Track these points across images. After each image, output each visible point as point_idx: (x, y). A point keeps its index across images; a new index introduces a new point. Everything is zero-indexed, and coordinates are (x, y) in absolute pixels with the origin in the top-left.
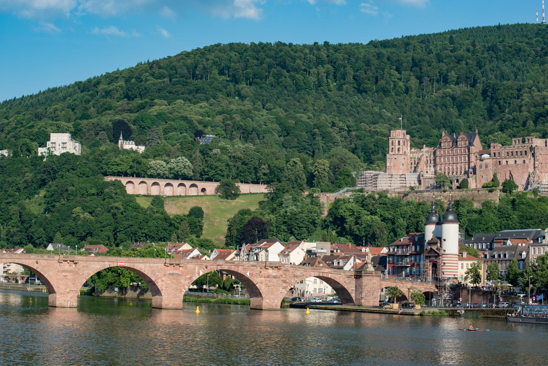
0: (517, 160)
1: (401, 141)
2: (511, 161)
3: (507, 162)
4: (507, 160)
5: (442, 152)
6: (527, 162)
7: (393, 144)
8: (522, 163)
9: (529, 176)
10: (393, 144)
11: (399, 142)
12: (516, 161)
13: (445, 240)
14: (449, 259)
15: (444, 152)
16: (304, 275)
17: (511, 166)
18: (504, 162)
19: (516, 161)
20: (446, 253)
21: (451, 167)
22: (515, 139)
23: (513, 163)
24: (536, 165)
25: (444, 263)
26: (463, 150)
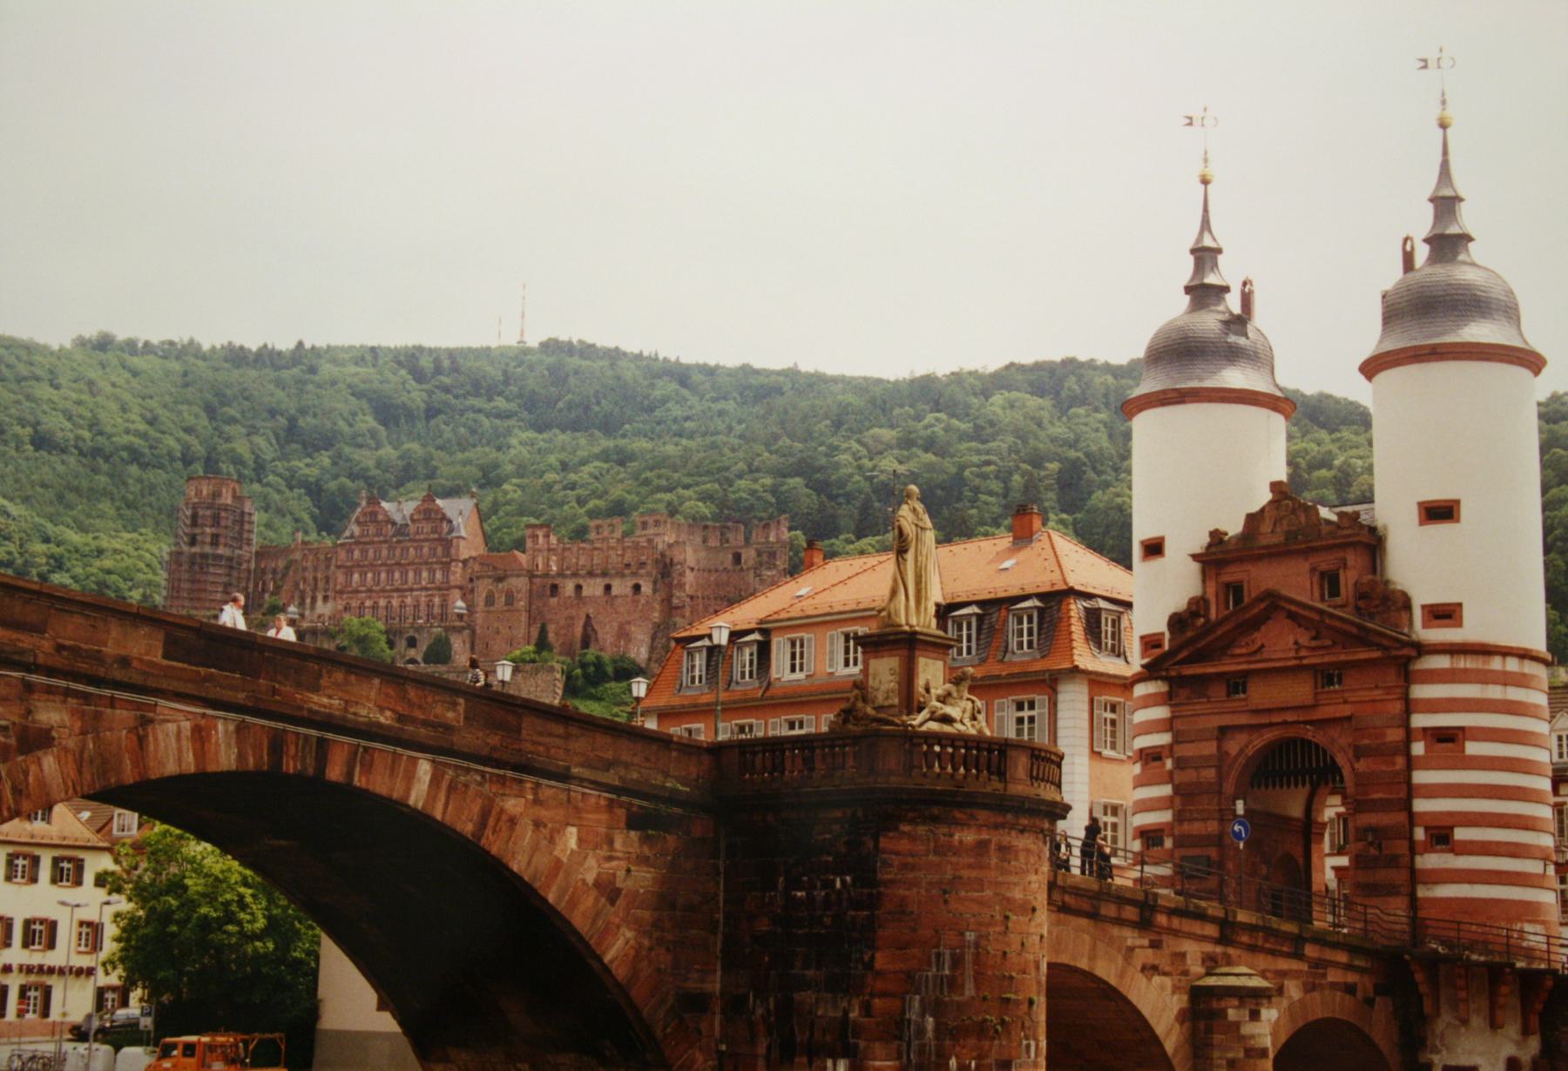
2: (593, 588)
3: (579, 588)
4: (581, 581)
5: (357, 554)
6: (646, 588)
8: (629, 591)
9: (653, 638)
12: (608, 588)
13: (1439, 512)
14: (1495, 692)
15: (364, 552)
17: (593, 599)
18: (569, 587)
19: (608, 588)
20: (1470, 631)
21: (382, 603)
23: (599, 591)
24: (675, 601)
25: (1447, 737)
26: (426, 550)
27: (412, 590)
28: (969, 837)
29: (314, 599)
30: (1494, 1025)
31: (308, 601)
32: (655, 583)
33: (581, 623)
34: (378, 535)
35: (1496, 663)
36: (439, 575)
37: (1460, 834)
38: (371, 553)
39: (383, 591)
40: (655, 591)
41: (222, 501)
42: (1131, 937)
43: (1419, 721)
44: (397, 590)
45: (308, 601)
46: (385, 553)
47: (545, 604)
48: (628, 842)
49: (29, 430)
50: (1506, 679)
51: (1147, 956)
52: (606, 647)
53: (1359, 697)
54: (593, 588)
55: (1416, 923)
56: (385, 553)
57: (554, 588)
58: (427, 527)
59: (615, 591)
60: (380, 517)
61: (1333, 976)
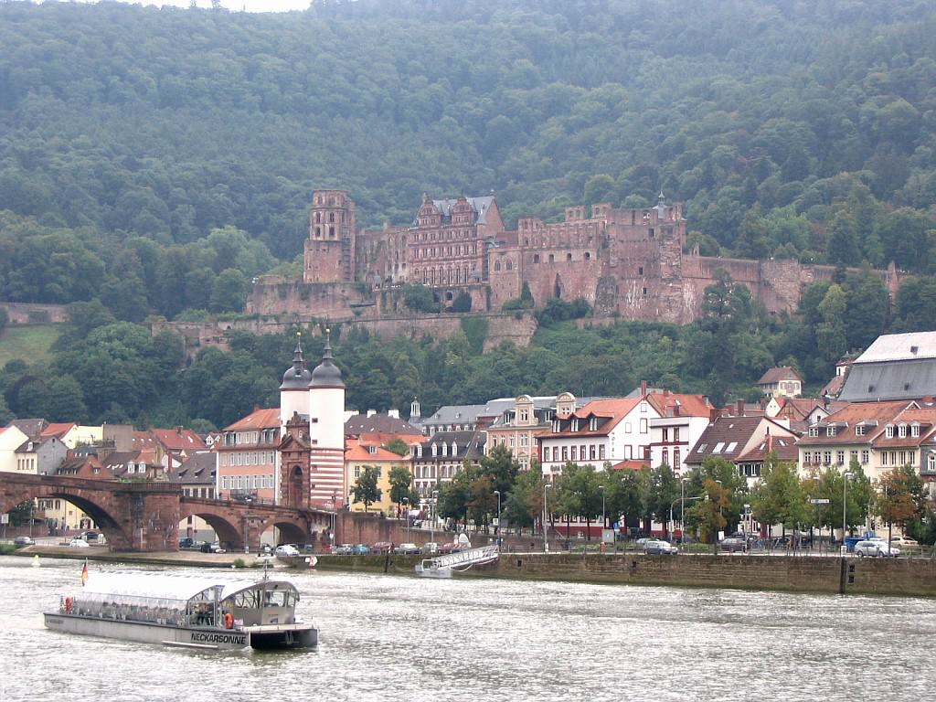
0: (574, 253)
1: (336, 214)
2: (560, 257)
4: (553, 253)
6: (593, 256)
7: (318, 221)
9: (597, 290)
10: (318, 221)
11: (332, 215)
13: (315, 421)
15: (425, 236)
16: (25, 492)
18: (545, 256)
19: (570, 256)
21: (437, 268)
22: (570, 209)
23: (564, 258)
25: (315, 466)
27: (455, 259)
28: (158, 497)
29: (397, 266)
30: (321, 524)
31: (393, 268)
32: (598, 252)
33: (554, 279)
34: (432, 224)
35: (324, 452)
36: (470, 249)
37: (316, 486)
38: (429, 237)
39: (438, 260)
40: (598, 256)
41: (336, 205)
42: (225, 508)
43: (312, 463)
44: (445, 260)
45: (393, 268)
46: (437, 235)
47: (532, 268)
48: (114, 498)
49: (258, 98)
50: (326, 455)
51: (230, 512)
52: (568, 296)
53: (304, 459)
54: (560, 257)
55: (309, 504)
56: (437, 235)
57: (537, 257)
58: (462, 217)
59: (573, 258)
60: (434, 212)
61: (285, 514)
